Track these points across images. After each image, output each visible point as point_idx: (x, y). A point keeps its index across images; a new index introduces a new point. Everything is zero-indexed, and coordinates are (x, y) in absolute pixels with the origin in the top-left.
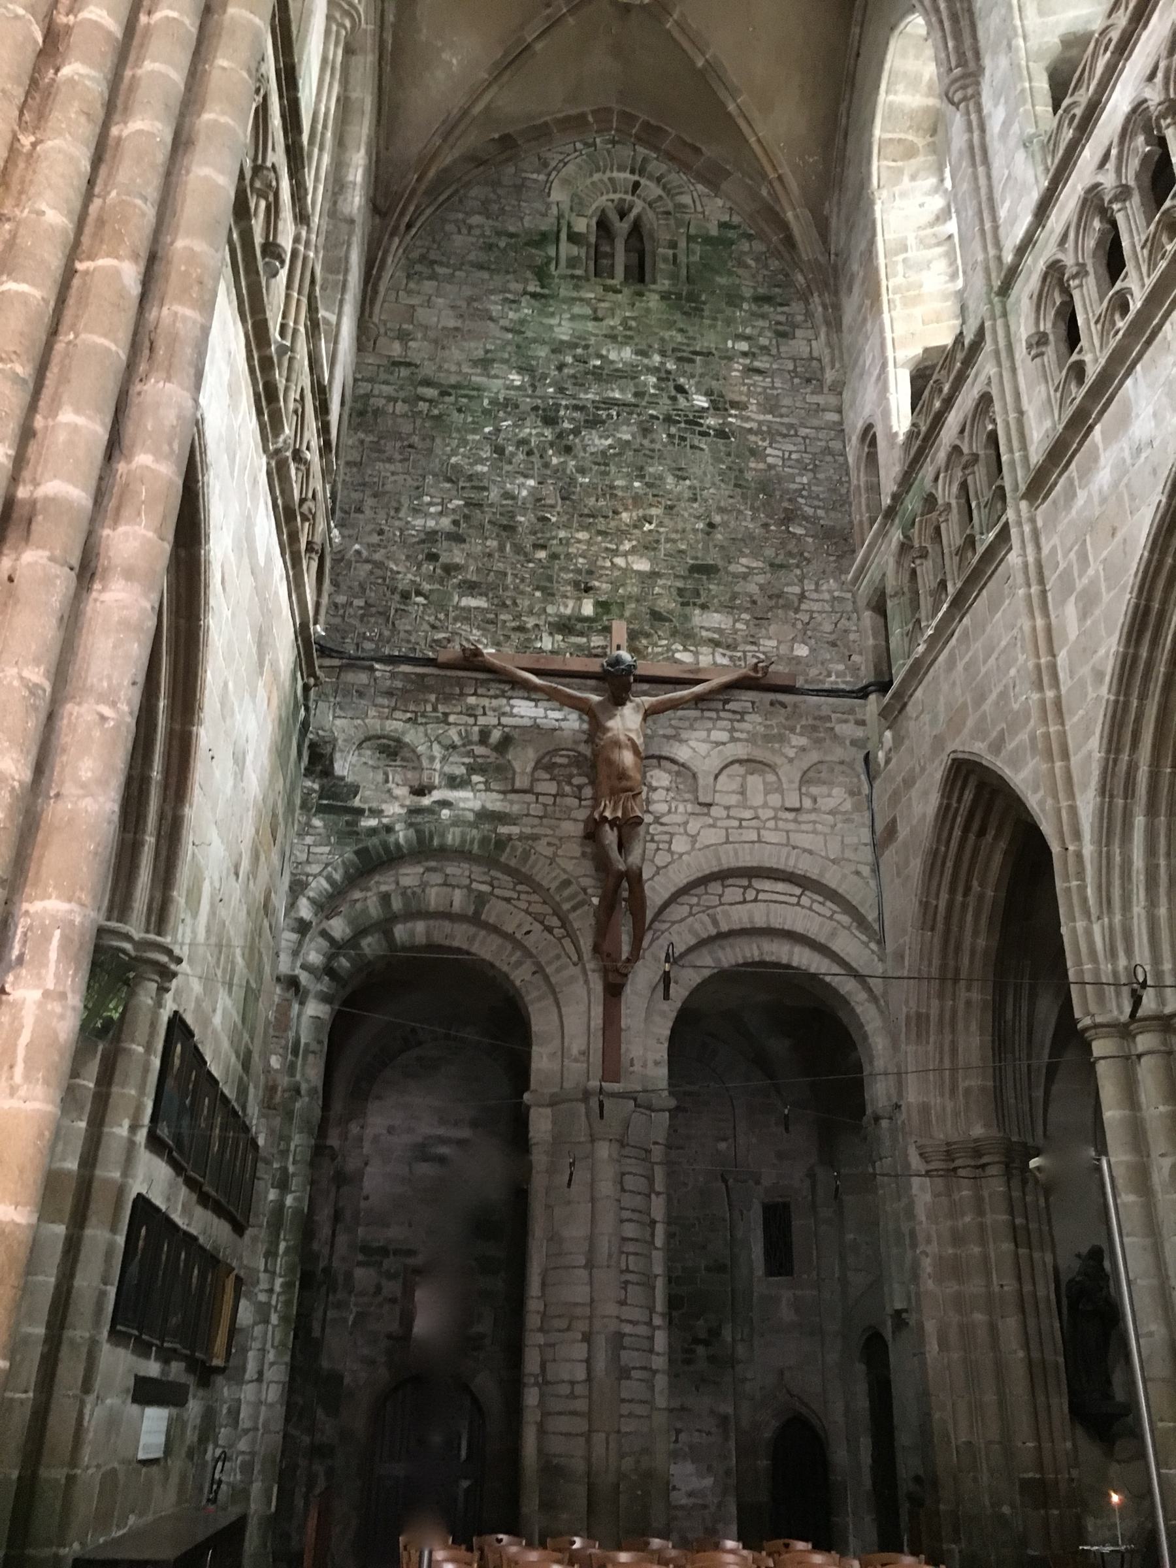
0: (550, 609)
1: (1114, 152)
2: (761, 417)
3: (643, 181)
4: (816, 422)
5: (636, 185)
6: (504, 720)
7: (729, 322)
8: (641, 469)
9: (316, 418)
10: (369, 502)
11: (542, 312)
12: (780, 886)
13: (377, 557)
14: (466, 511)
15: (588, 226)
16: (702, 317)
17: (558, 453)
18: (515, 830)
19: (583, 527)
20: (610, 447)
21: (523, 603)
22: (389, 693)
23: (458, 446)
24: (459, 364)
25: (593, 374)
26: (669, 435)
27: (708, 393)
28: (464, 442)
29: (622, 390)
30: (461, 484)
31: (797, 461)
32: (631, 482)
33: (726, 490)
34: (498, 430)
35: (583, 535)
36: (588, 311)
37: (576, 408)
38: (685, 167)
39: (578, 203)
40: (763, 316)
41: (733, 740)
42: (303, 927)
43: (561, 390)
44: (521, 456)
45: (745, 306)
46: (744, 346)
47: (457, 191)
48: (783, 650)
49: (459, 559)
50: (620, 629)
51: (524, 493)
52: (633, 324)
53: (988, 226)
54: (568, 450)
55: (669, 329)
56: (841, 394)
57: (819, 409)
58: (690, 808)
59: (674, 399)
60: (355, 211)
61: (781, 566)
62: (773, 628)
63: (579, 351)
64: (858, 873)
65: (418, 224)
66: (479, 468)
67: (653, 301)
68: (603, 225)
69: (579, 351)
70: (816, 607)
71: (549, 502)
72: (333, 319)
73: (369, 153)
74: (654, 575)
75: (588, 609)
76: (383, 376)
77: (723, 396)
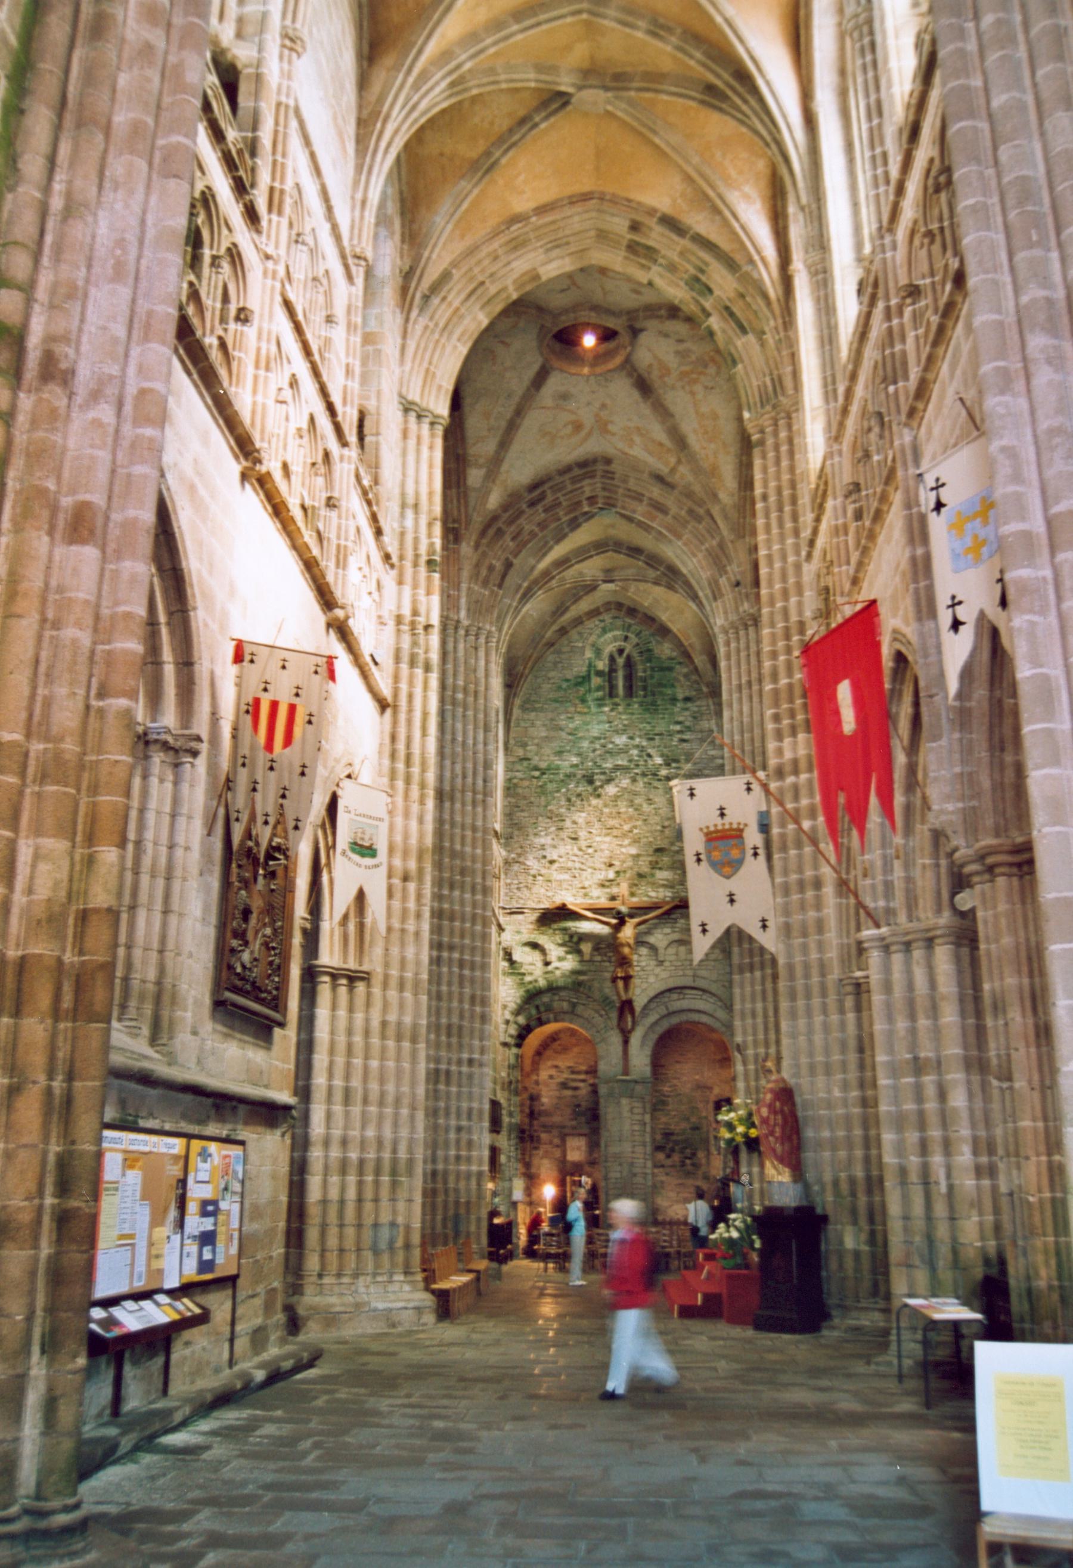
5: (626, 638)
42: (507, 1022)
46: (678, 728)
57: (713, 758)
68: (612, 659)
74: (638, 856)
75: (611, 875)
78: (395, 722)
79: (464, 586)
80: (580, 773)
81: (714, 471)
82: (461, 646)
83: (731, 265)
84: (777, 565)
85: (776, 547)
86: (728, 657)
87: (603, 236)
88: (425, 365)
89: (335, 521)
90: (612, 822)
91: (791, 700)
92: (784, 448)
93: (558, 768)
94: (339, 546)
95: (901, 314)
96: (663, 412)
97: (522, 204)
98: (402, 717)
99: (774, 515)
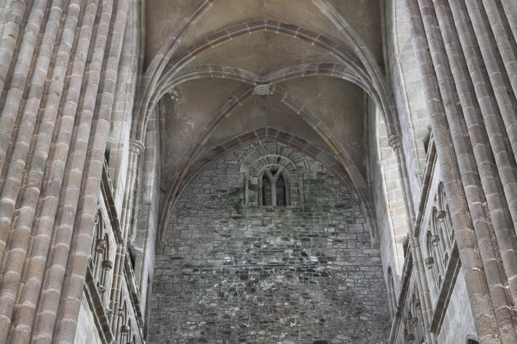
1: (437, 197)
2: (343, 264)
3: (282, 157)
4: (369, 263)
5: (279, 159)
7: (324, 219)
8: (288, 296)
9: (133, 306)
10: (163, 327)
11: (239, 226)
14: (207, 326)
15: (258, 180)
16: (312, 218)
17: (249, 293)
19: (263, 328)
20: (273, 287)
23: (202, 295)
24: (202, 255)
25: (263, 252)
26: (300, 278)
27: (317, 254)
28: (205, 293)
29: (277, 258)
30: (204, 314)
31: (361, 283)
32: (284, 303)
33: (329, 302)
34: (220, 285)
35: (262, 332)
36: (259, 222)
37: (256, 270)
38: (300, 150)
39: (253, 172)
40: (340, 214)
43: (249, 261)
44: (232, 297)
45: (332, 211)
47: (198, 175)
51: (234, 314)
52: (280, 225)
53: (409, 204)
54: (253, 291)
55: (297, 226)
56: (379, 248)
57: (369, 256)
59: (301, 259)
60: (151, 199)
61: (357, 338)
63: (256, 242)
65: (181, 193)
66: (213, 305)
67: (289, 214)
68: (265, 177)
69: (256, 242)
71: (246, 317)
72: (142, 250)
73: (157, 172)
77: (324, 255)
80: (233, 270)
90: (266, 316)
93: (211, 266)
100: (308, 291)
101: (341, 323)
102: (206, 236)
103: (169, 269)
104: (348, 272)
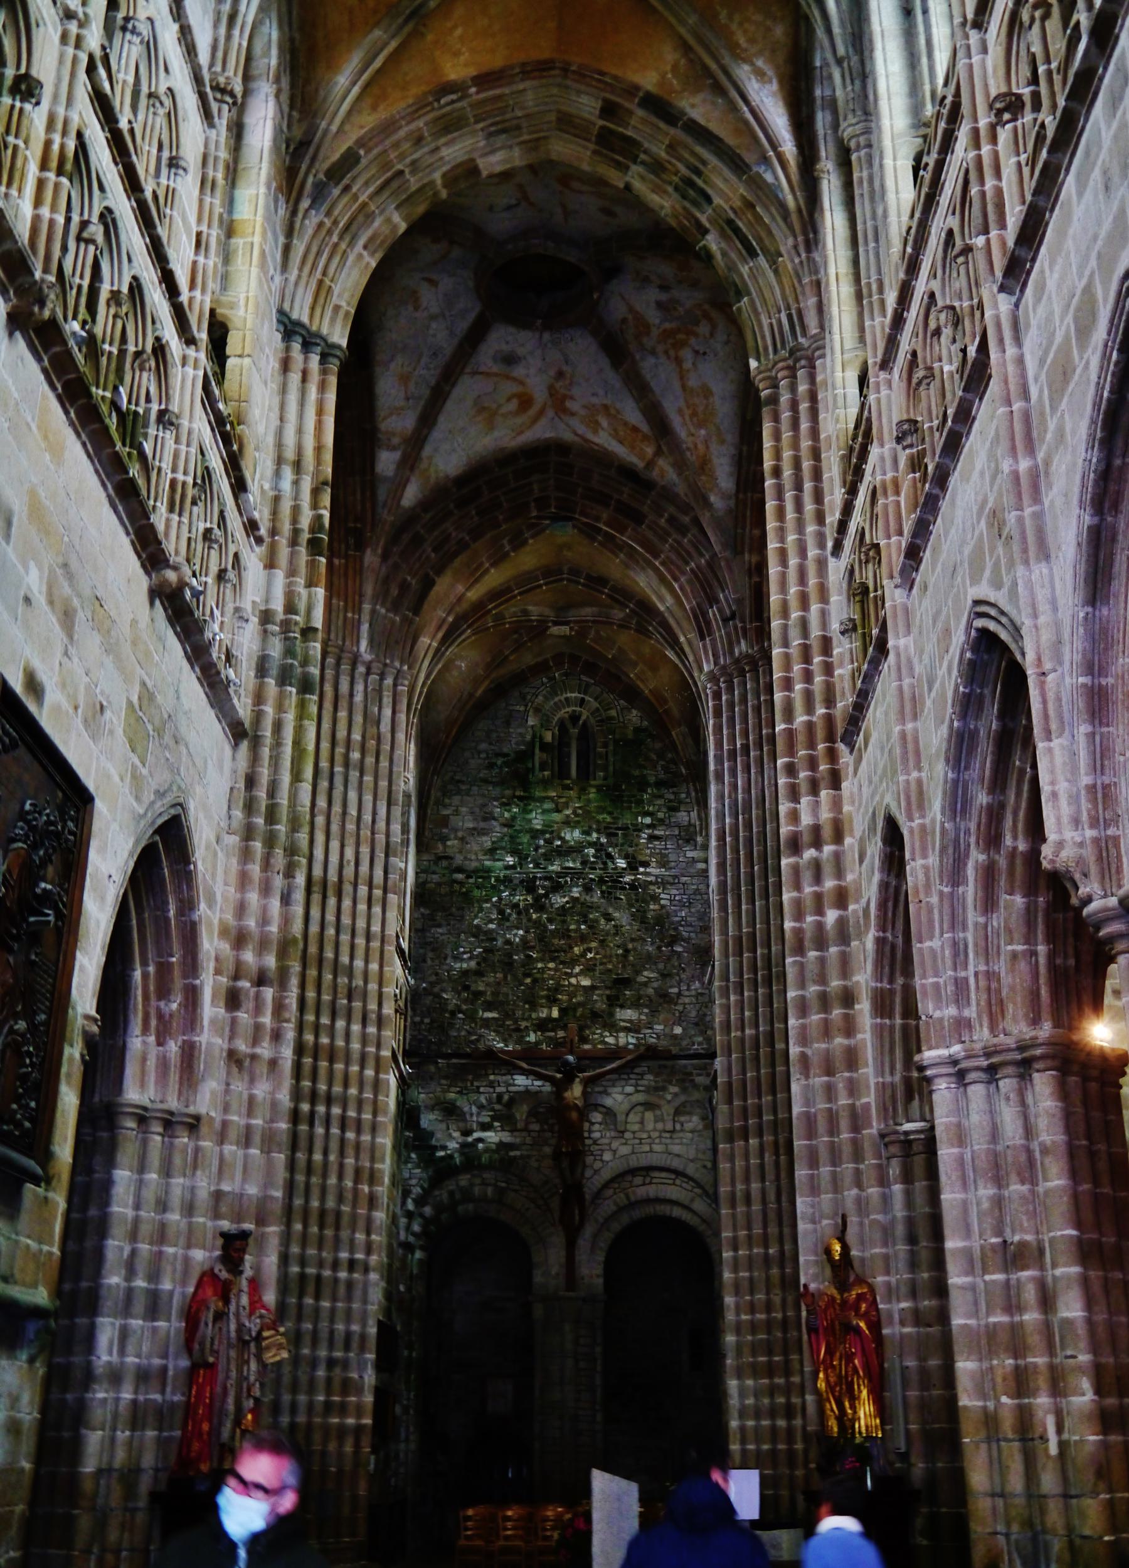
0: (534, 1015)
3: (587, 698)
6: (512, 1089)
10: (430, 955)
12: (664, 1175)
13: (436, 990)
18: (518, 1153)
19: (553, 960)
21: (519, 1013)
22: (446, 1077)
27: (626, 857)
28: (481, 909)
29: (574, 861)
34: (500, 899)
35: (551, 965)
37: (545, 878)
39: (545, 724)
40: (661, 797)
41: (637, 1091)
42: (409, 1215)
43: (537, 866)
46: (648, 820)
48: (667, 1030)
49: (481, 988)
50: (573, 1026)
57: (694, 861)
58: (613, 1134)
62: (662, 1017)
64: (705, 1167)
66: (492, 926)
70: (687, 1000)
72: (402, 865)
74: (593, 988)
76: (434, 868)
78: (255, 759)
79: (367, 607)
80: (517, 876)
81: (705, 464)
82: (359, 688)
83: (738, 165)
84: (793, 561)
85: (791, 538)
86: (718, 713)
87: (567, 123)
88: (318, 274)
89: (170, 444)
90: (557, 942)
91: (812, 745)
92: (804, 406)
93: (489, 870)
94: (173, 483)
95: (994, 139)
96: (640, 389)
97: (455, 70)
98: (266, 752)
99: (789, 495)
100: (611, 910)
101: (649, 955)
102: (482, 825)
103: (434, 873)
104: (663, 883)
